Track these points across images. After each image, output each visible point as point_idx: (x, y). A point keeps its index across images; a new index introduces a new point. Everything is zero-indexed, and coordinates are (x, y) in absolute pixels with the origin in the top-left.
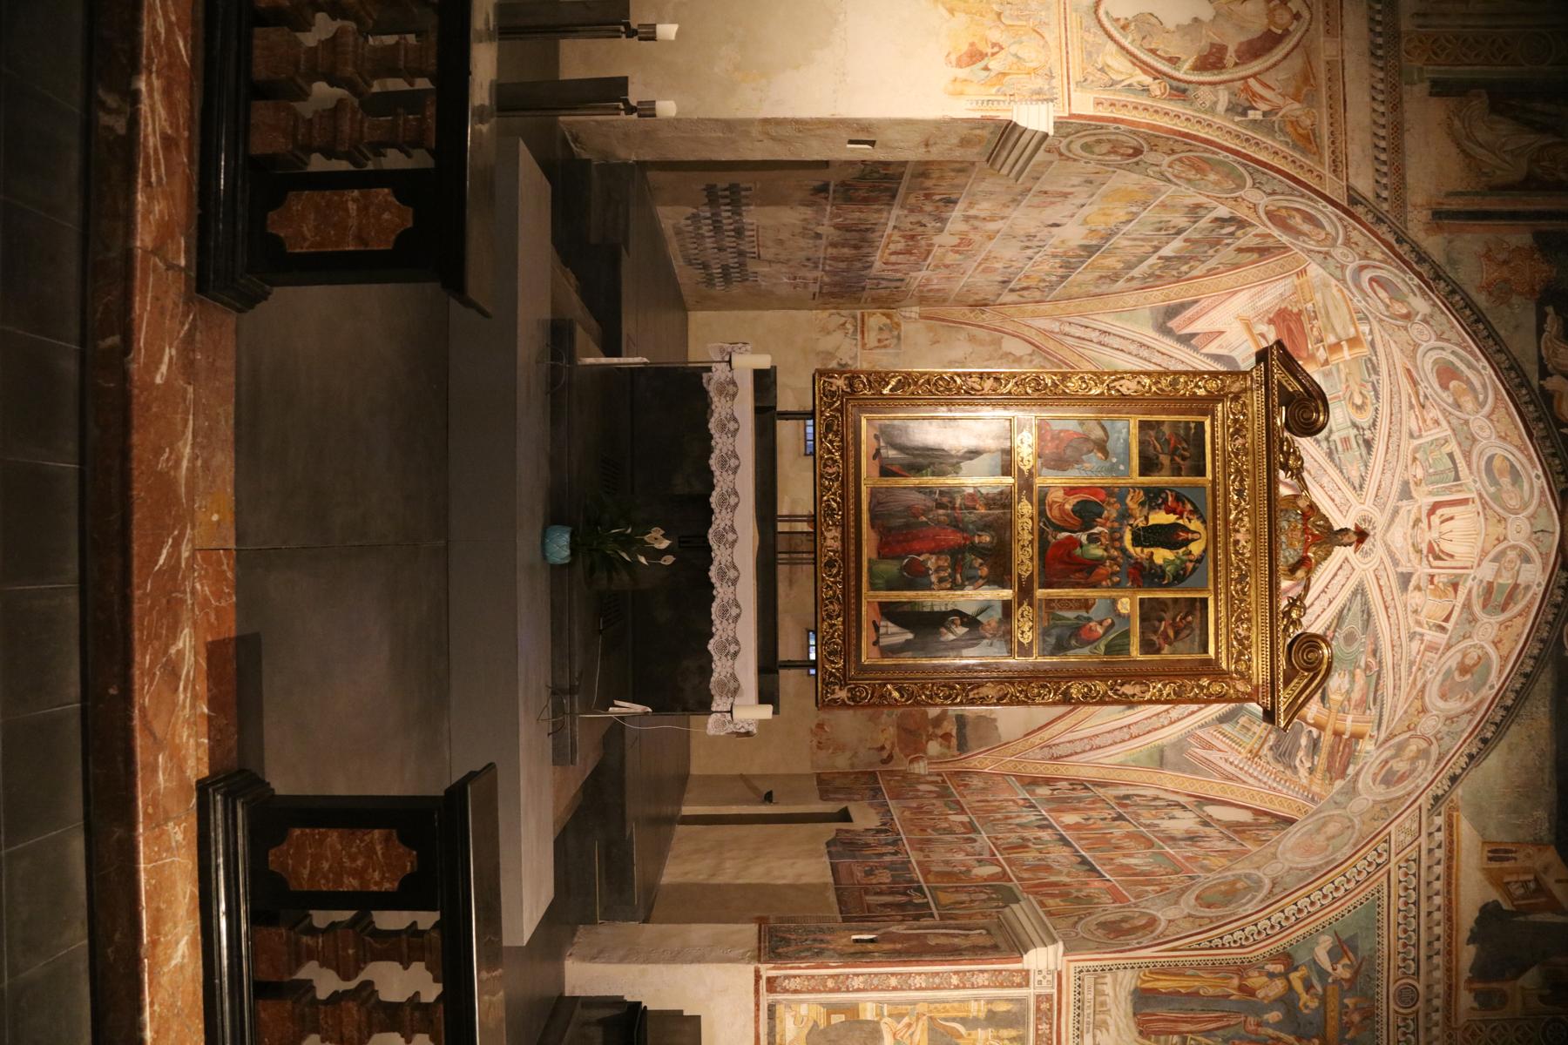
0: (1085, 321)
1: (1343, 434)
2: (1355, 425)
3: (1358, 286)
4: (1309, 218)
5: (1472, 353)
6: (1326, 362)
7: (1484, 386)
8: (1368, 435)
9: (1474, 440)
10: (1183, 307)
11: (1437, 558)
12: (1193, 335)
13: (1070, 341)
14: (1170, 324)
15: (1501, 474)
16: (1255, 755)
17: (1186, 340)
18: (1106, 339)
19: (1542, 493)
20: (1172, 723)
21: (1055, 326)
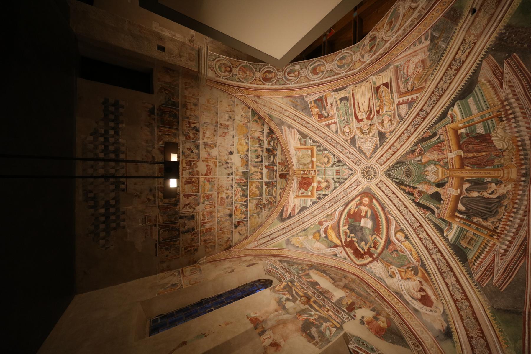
0: (263, 236)
1: (335, 173)
2: (333, 166)
3: (288, 80)
4: (270, 72)
5: (312, 61)
6: (315, 171)
7: (320, 61)
8: (336, 160)
9: (332, 70)
10: (282, 211)
11: (371, 113)
12: (290, 214)
13: (263, 246)
14: (283, 217)
15: (342, 63)
16: (493, 232)
17: (290, 217)
18: (272, 237)
19: (348, 49)
20: (467, 299)
21: (256, 244)
